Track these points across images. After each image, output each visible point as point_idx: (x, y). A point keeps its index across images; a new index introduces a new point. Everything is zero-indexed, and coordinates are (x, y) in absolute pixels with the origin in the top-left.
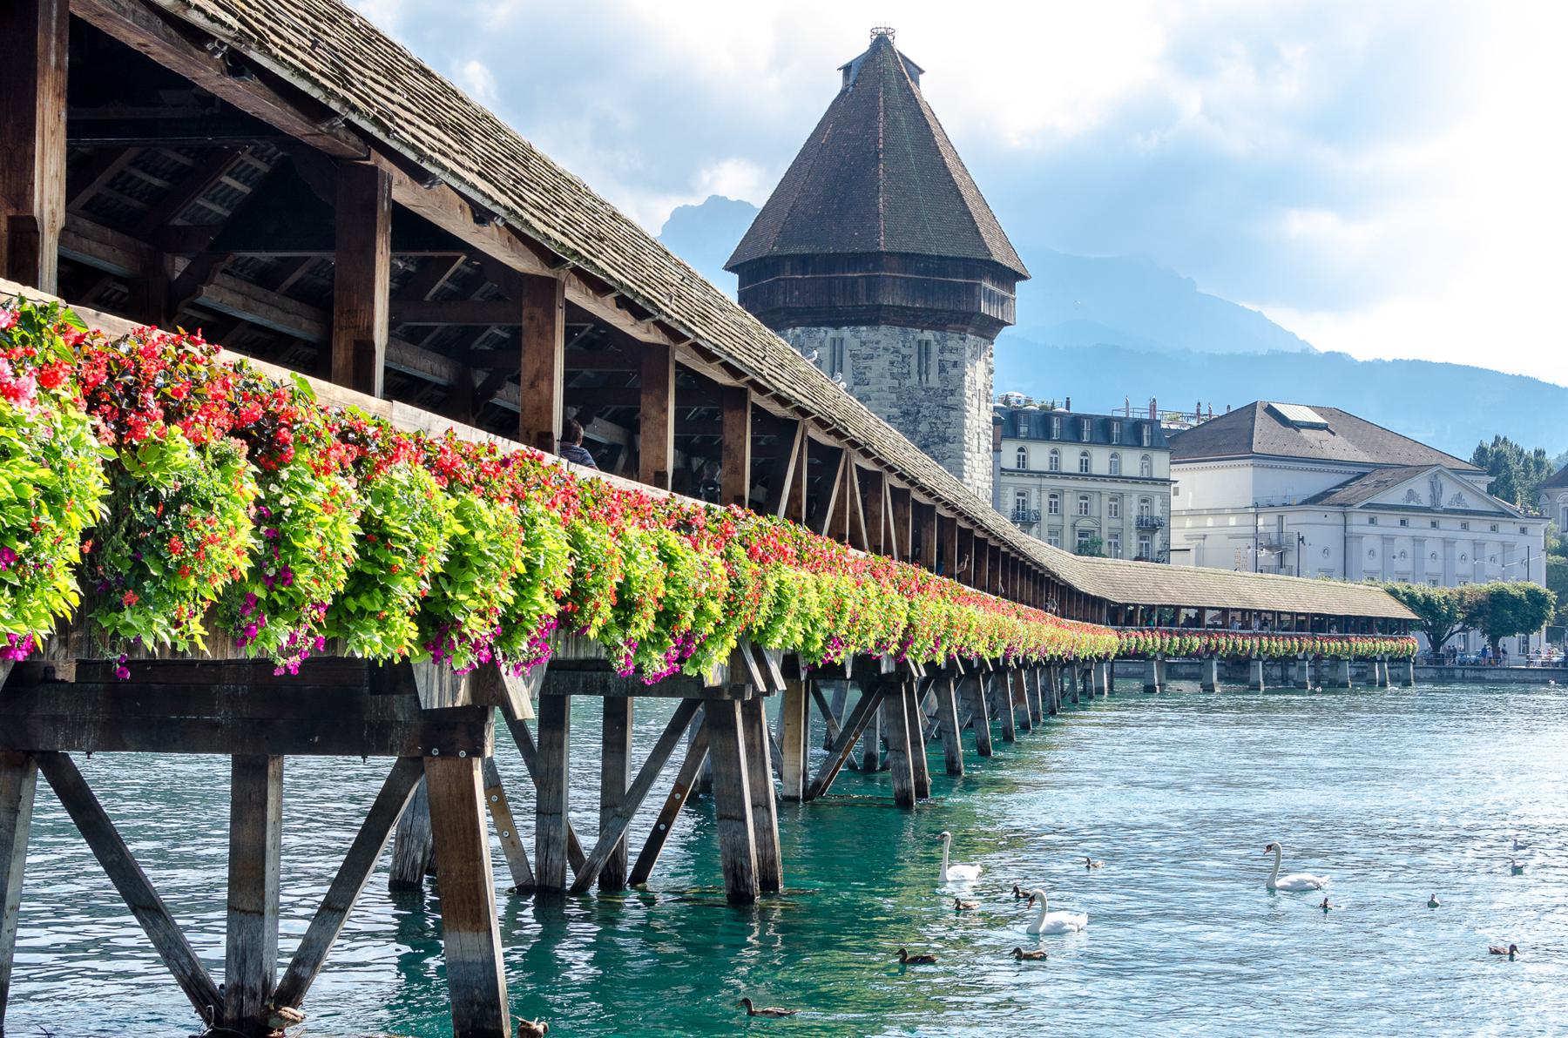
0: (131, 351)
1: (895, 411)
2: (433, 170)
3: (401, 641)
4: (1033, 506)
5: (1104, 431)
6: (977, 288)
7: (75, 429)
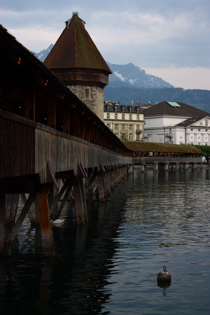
6: (100, 76)
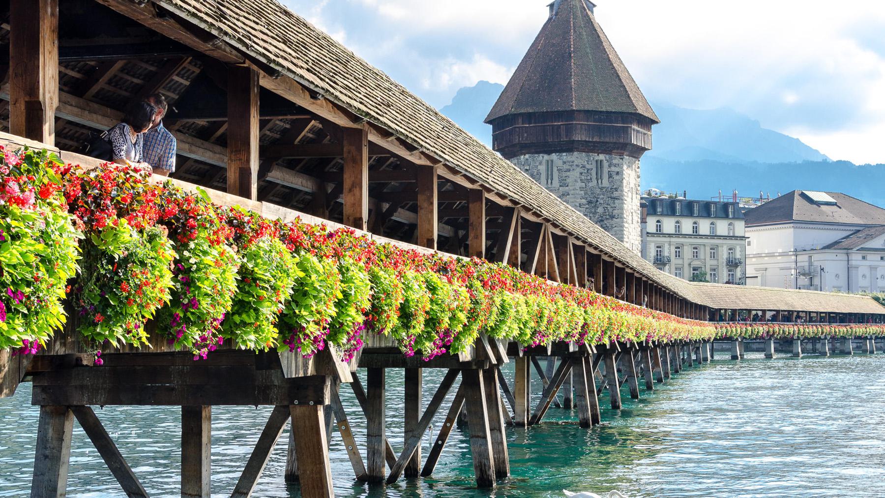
0: (97, 176)
1: (584, 201)
2: (277, 68)
3: (268, 339)
4: (666, 254)
5: (706, 210)
6: (629, 129)
7: (61, 222)
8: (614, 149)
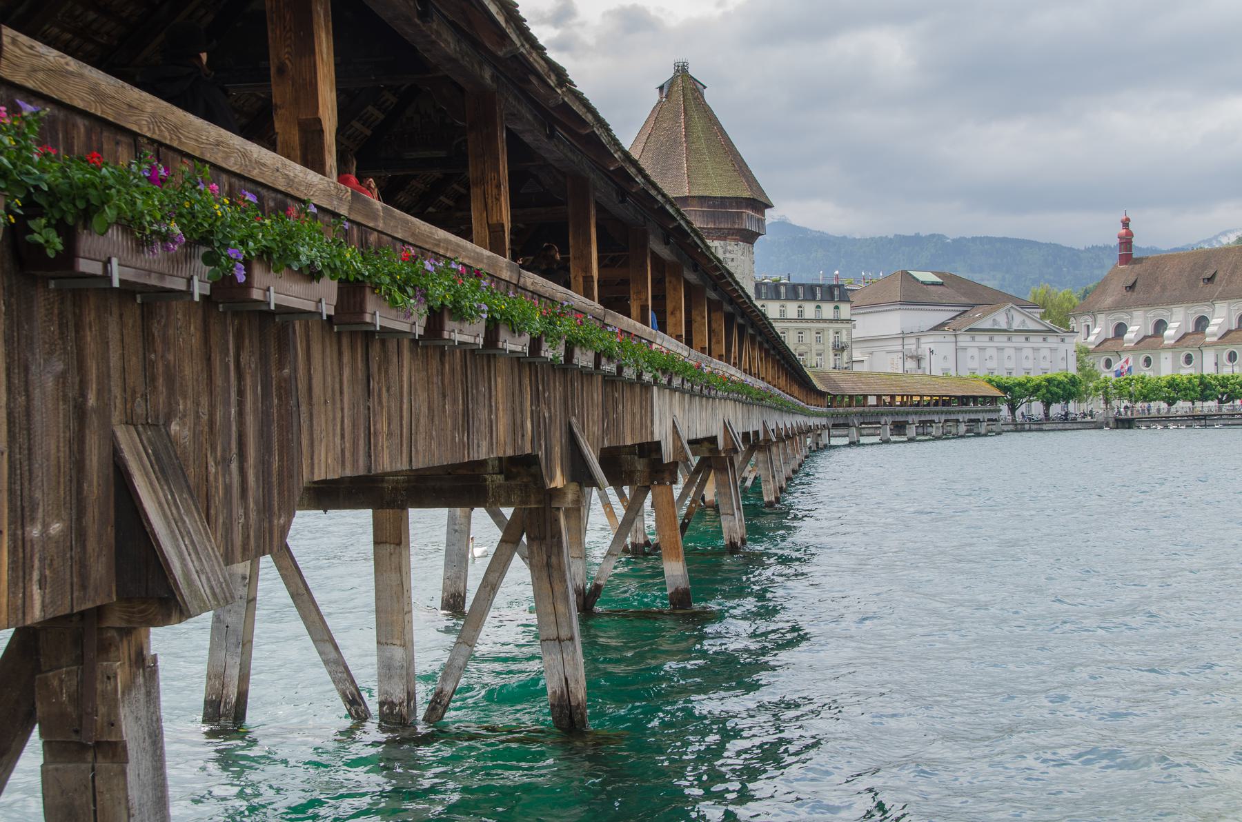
8: (729, 234)
